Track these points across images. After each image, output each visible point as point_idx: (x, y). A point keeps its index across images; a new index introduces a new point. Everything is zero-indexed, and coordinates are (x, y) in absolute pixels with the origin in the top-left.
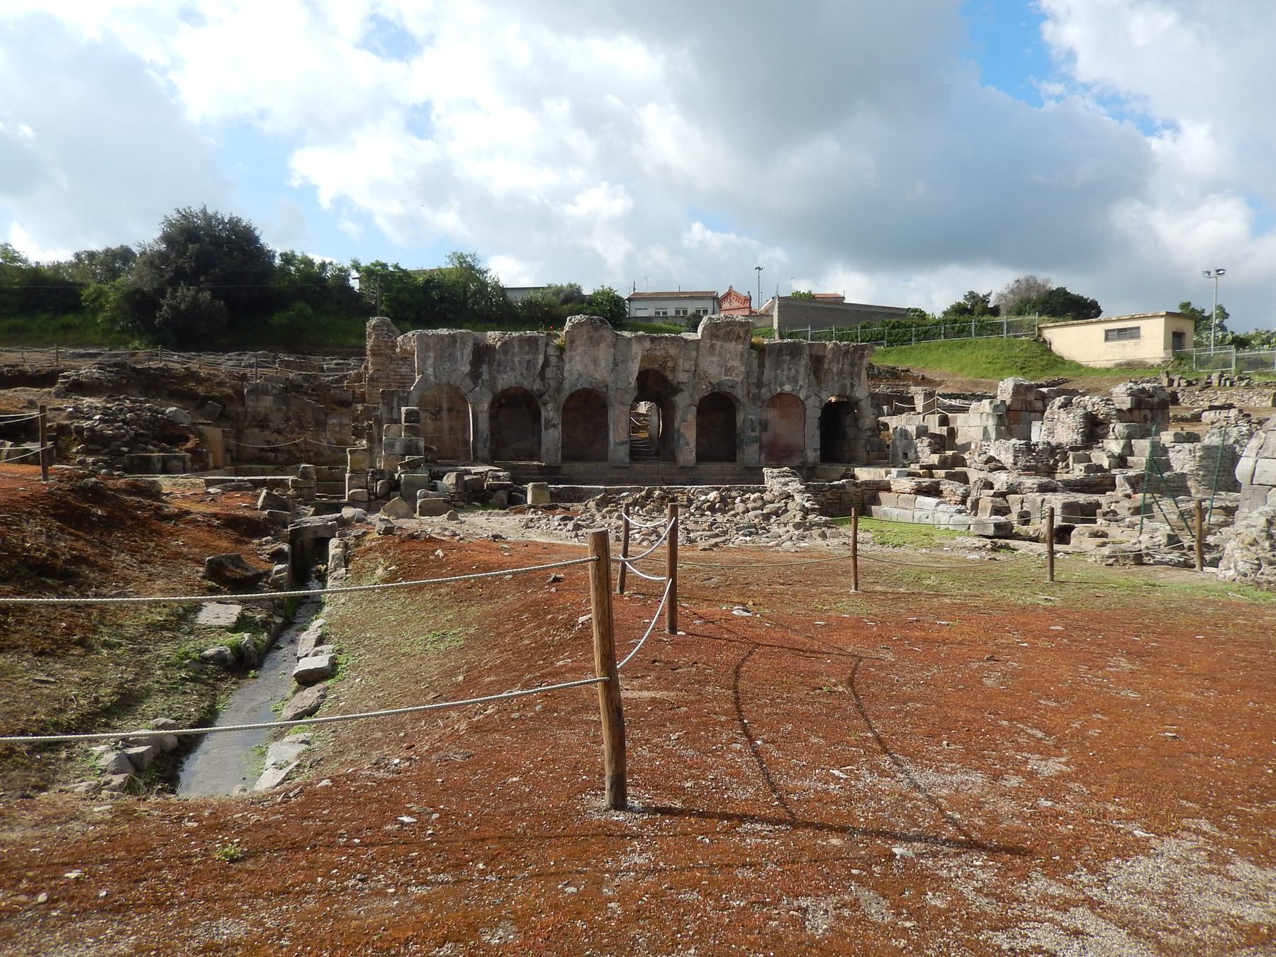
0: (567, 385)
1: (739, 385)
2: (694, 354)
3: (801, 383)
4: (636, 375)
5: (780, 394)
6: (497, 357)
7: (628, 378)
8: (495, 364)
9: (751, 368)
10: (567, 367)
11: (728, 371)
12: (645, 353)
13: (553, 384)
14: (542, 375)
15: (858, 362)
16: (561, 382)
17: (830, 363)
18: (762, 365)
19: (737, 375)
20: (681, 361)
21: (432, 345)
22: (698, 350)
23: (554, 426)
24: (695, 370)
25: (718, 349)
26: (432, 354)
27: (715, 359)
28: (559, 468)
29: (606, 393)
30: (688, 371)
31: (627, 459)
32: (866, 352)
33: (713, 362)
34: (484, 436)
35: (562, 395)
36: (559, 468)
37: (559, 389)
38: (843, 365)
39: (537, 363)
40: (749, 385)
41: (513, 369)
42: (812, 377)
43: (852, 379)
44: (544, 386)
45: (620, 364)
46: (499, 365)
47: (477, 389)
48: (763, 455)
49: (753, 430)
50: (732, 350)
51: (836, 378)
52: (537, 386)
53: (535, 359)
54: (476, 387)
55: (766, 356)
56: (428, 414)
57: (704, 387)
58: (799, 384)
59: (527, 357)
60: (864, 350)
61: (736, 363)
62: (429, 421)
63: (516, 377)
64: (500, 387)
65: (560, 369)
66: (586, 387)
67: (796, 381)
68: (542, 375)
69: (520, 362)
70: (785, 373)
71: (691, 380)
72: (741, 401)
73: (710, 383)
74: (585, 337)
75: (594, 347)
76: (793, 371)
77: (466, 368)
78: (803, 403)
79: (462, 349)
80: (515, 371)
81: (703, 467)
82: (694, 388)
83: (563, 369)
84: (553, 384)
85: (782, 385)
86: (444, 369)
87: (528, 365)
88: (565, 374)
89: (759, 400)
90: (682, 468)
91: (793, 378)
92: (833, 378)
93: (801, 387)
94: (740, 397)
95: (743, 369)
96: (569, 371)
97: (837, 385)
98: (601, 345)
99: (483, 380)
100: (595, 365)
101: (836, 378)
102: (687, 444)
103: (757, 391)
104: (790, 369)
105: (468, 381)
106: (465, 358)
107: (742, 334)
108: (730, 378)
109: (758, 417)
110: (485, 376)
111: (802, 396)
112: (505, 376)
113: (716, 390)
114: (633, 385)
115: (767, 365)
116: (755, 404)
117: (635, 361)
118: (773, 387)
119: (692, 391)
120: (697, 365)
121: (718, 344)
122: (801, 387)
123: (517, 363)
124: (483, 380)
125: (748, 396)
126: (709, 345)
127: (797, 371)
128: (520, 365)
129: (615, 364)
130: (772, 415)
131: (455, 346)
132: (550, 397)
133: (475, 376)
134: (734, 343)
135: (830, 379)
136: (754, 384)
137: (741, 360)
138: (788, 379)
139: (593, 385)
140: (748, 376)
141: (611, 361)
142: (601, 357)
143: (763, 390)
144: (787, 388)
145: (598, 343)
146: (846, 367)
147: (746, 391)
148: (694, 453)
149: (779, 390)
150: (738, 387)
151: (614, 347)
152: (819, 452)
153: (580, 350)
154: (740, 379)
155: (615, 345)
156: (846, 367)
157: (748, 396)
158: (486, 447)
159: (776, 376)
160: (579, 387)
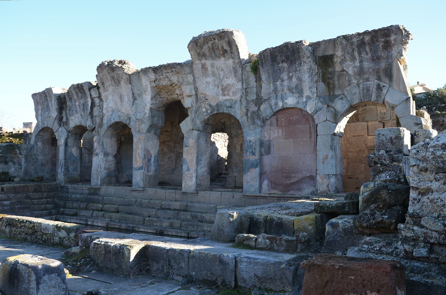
0: (105, 121)
1: (238, 104)
2: (190, 78)
3: (307, 93)
4: (148, 106)
5: (284, 109)
6: (68, 104)
7: (144, 110)
8: (68, 108)
9: (248, 84)
10: (105, 106)
11: (225, 90)
12: (154, 85)
13: (98, 120)
14: (91, 113)
15: (383, 54)
16: (102, 119)
17: (342, 63)
18: (258, 80)
19: (234, 93)
20: (183, 88)
21: (38, 100)
22: (192, 72)
23: (97, 155)
24: (196, 94)
25: (209, 69)
26: (40, 107)
27: (209, 79)
28: (99, 189)
29: (129, 124)
30: (190, 96)
31: (142, 184)
32: (393, 37)
33: (208, 83)
34: (62, 164)
35: (102, 129)
36: (99, 189)
37: (101, 125)
38: (361, 62)
39: (88, 105)
40: (248, 102)
41: (77, 112)
42: (322, 85)
43: (379, 79)
44: (92, 122)
45: (137, 98)
46: (70, 110)
47: (60, 129)
48: (266, 183)
49: (254, 154)
50: (223, 66)
51: (355, 82)
52: (88, 123)
53: (86, 102)
54: (60, 127)
55: (260, 67)
56: (87, 151)
57: (204, 110)
58: (305, 95)
59: (82, 101)
60: (389, 36)
61: (231, 80)
62: (87, 155)
63: (78, 118)
64: (71, 127)
65: (101, 107)
66: (117, 120)
67: (300, 92)
68: (91, 113)
69: (79, 106)
70: (286, 83)
71: (194, 105)
72: (240, 121)
73: (210, 105)
74: (109, 78)
75: (118, 86)
76: (294, 80)
77: (54, 114)
78: (312, 117)
79: (51, 101)
80: (77, 113)
81: (201, 193)
82: (196, 112)
83: (103, 107)
84: (98, 120)
85: (282, 99)
86: (45, 116)
87: (83, 107)
88: (104, 112)
89: (260, 119)
90: (184, 193)
91: (296, 87)
92: (349, 81)
93: (308, 98)
94: (238, 117)
95: (239, 86)
96: (106, 108)
97: (356, 90)
98: (122, 83)
99: (63, 122)
100: (122, 102)
101: (355, 82)
102: (188, 170)
103: (256, 108)
104: (290, 78)
105: (56, 124)
106: (53, 107)
107: (226, 47)
108: (227, 97)
109: (258, 136)
110: (64, 120)
111: (309, 109)
112: (73, 118)
113: (216, 112)
114: (147, 115)
115: (264, 77)
116: (254, 123)
117: (147, 93)
118: (273, 102)
119: (193, 117)
120: (196, 89)
121: (208, 63)
122: (308, 98)
123: (78, 107)
124: (63, 122)
125: (247, 115)
126: (200, 66)
127: (300, 79)
128: (79, 108)
129: (135, 99)
130: (276, 135)
131: (47, 100)
132: (95, 132)
133: (60, 119)
134: (223, 59)
135: (347, 84)
136: (253, 100)
137: (236, 76)
138: (290, 90)
139: (122, 118)
140: (247, 92)
141: (131, 96)
142: (125, 94)
143: (262, 107)
144: (291, 101)
145: (120, 83)
146: (366, 65)
147: (245, 110)
148: (194, 178)
149: (280, 104)
150: (237, 106)
151: (130, 83)
152: (333, 180)
153: (111, 89)
154: (238, 97)
155: (130, 80)
156: (366, 65)
157: (247, 115)
158: (62, 172)
159: (275, 90)
160: (113, 121)
